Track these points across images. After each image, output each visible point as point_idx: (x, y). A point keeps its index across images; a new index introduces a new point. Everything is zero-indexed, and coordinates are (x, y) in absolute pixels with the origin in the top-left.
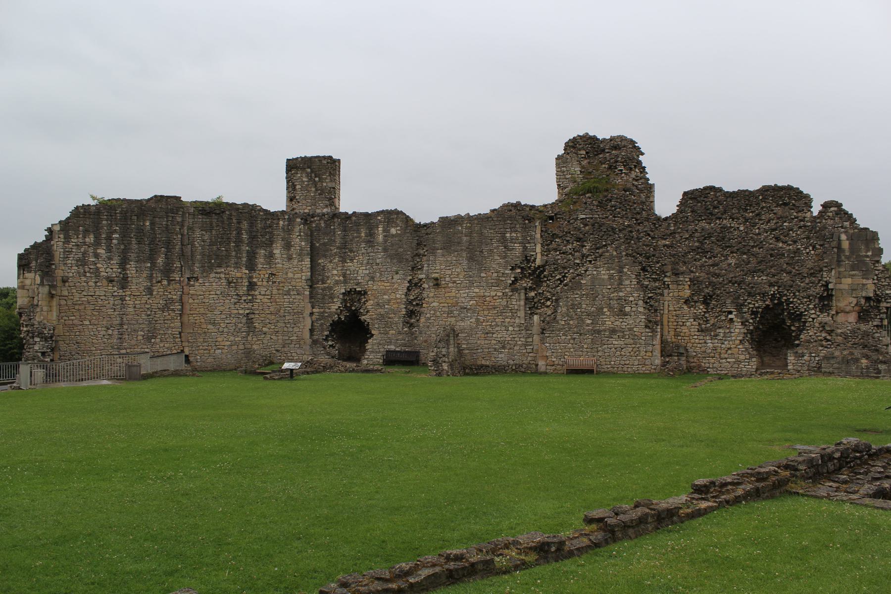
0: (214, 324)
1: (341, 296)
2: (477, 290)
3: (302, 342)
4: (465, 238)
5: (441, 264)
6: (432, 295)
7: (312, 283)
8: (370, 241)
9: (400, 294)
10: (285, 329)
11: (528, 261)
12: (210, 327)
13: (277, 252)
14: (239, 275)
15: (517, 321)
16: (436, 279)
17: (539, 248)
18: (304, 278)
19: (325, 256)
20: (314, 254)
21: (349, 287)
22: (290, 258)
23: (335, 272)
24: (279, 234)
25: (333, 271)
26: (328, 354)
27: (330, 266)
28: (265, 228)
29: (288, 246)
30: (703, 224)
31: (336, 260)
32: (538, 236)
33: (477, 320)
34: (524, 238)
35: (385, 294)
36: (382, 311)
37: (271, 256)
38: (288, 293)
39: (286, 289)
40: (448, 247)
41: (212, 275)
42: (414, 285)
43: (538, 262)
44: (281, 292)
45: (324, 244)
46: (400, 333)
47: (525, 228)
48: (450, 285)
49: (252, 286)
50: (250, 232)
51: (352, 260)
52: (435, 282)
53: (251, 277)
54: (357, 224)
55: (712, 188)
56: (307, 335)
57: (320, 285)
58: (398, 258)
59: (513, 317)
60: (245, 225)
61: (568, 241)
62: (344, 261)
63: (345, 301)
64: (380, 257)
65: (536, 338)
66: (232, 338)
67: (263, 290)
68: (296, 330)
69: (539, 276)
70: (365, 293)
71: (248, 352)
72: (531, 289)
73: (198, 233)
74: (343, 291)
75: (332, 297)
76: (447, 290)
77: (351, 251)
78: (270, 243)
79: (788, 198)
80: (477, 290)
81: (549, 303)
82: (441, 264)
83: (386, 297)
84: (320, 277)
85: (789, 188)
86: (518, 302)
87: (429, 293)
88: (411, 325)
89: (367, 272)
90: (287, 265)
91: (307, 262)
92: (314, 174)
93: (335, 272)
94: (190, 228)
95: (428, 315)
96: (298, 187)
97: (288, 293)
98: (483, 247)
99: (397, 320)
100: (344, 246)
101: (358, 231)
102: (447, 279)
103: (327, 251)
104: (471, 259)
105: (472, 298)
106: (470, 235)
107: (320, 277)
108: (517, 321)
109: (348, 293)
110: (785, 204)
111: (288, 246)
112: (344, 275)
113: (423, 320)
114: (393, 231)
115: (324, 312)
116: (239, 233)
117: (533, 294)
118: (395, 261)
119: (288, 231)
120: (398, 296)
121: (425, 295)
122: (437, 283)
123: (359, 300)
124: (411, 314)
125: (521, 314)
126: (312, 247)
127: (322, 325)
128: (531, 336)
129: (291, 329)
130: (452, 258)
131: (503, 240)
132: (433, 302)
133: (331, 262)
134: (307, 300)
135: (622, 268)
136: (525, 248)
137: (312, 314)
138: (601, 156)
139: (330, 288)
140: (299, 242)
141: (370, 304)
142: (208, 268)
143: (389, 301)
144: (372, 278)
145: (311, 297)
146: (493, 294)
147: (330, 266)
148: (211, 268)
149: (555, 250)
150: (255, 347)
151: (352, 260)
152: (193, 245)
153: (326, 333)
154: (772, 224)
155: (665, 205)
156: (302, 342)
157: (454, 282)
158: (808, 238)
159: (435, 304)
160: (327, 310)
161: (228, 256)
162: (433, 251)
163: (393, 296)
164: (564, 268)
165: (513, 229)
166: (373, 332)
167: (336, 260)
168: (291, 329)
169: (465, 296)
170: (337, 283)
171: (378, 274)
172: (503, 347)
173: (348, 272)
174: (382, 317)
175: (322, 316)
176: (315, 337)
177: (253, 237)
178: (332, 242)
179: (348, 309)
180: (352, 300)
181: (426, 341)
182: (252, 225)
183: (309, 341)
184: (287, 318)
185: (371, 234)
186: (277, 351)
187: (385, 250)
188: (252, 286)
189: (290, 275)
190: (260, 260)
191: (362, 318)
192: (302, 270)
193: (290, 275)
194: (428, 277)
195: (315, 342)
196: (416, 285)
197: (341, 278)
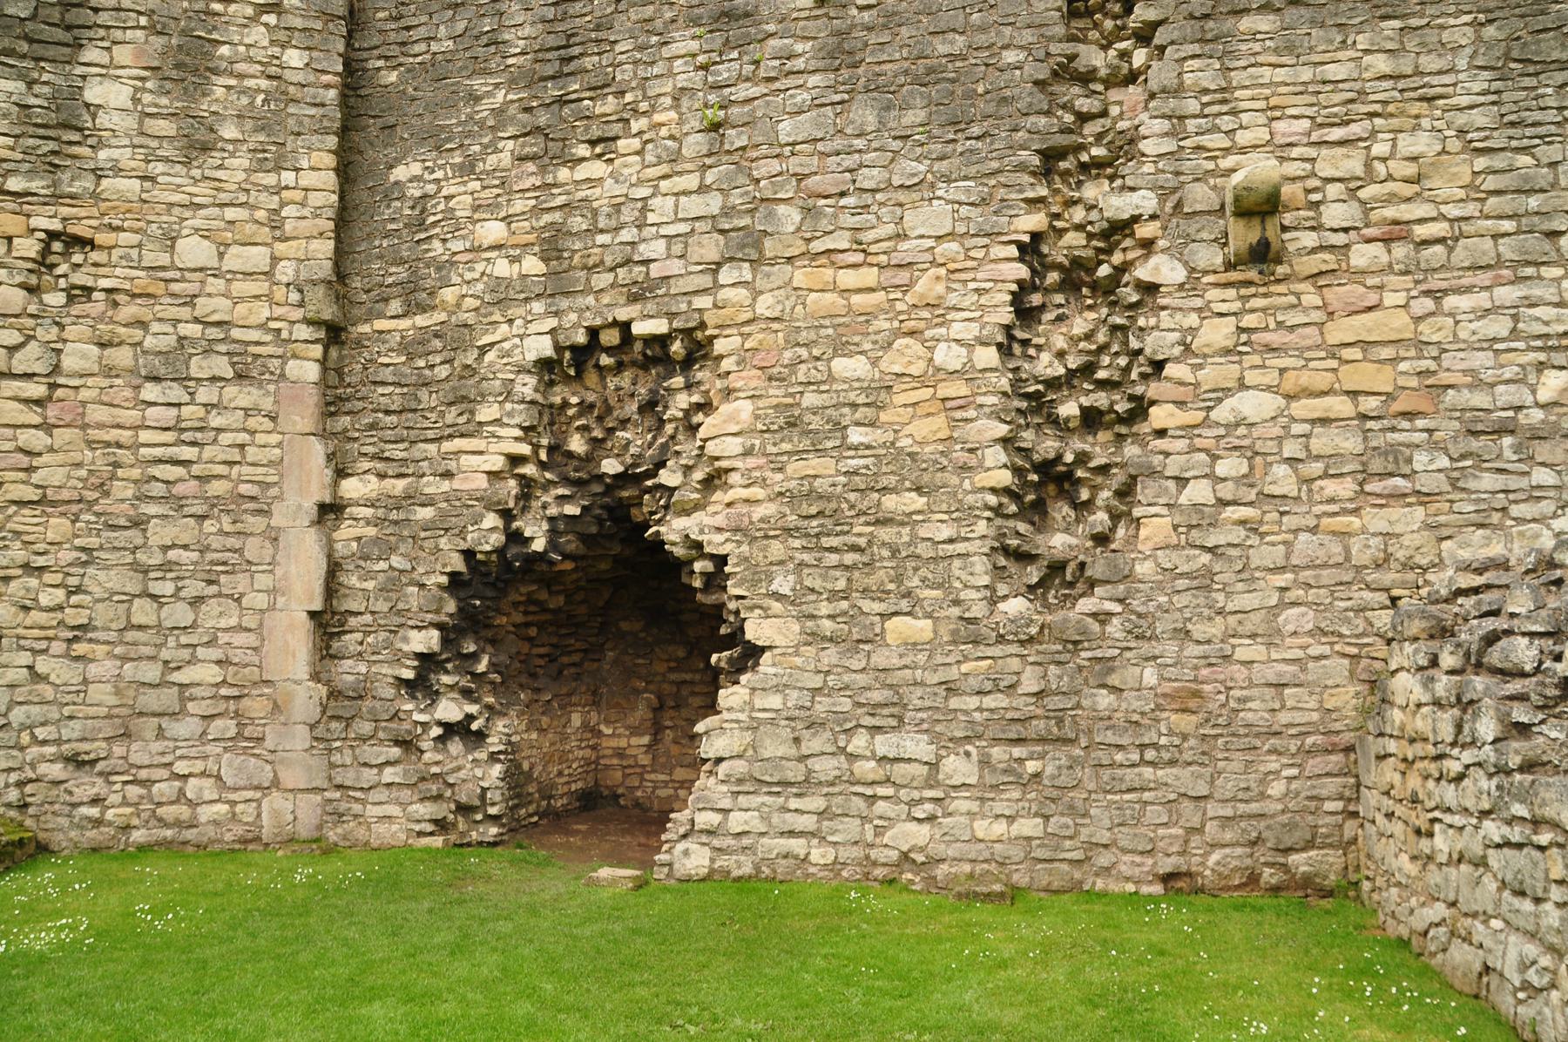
1: (527, 386)
3: (256, 706)
5: (1274, 113)
6: (1217, 333)
9: (965, 342)
10: (143, 612)
13: (110, 96)
18: (286, 271)
19: (436, 140)
20: (359, 125)
22: (198, 145)
23: (493, 231)
26: (430, 785)
27: (462, 195)
29: (188, 63)
35: (842, 348)
38: (171, 368)
39: (159, 339)
42: (1070, 273)
44: (122, 357)
45: (436, 70)
46: (970, 633)
48: (1363, 255)
51: (603, 144)
52: (1243, 235)
57: (393, 324)
62: (549, 149)
63: (551, 416)
68: (216, 616)
70: (699, 350)
76: (1344, 293)
82: (1274, 113)
83: (850, 367)
84: (401, 273)
89: (714, 203)
90: (175, 184)
91: (315, 174)
93: (493, 231)
95: (1199, 492)
97: (171, 368)
102: (1335, 214)
107: (401, 273)
109: (574, 361)
111: (188, 63)
112: (552, 246)
113: (1156, 527)
115: (412, 498)
118: (914, 116)
120: (948, 356)
122: (1260, 233)
124: (1045, 485)
126: (353, 78)
129: (180, 614)
133: (467, 169)
134: (302, 417)
137: (330, 511)
139: (456, 337)
141: (727, 430)
143: (878, 392)
144: (747, 246)
145: (335, 398)
147: (462, 195)
151: (603, 144)
153: (426, 640)
156: (256, 706)
157: (1396, 232)
159: (1254, 405)
160: (433, 486)
163: (906, 356)
166: (754, 631)
168: (180, 614)
170: (502, 296)
171: (789, 216)
173: (578, 223)
174: (817, 518)
176: (348, 671)
179: (578, 475)
181: (1187, 699)
183: (306, 698)
184: (159, 533)
186: (76, 762)
189: (194, 251)
191: (673, 530)
192: (275, 222)
193: (194, 251)
195: (341, 704)
196: (1076, 276)
197: (533, 265)
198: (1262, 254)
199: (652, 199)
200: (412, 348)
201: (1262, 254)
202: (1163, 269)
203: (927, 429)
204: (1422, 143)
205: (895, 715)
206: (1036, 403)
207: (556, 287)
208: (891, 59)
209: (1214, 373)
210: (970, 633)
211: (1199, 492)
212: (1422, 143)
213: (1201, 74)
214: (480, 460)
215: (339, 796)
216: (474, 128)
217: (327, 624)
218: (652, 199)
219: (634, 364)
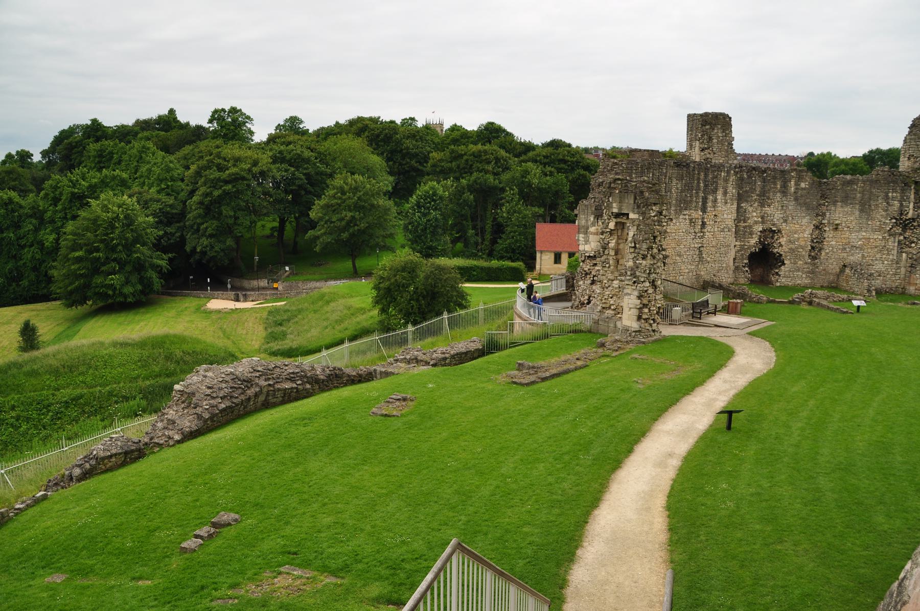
0: (680, 256)
4: (859, 195)
7: (738, 220)
8: (784, 191)
9: (807, 234)
11: (901, 214)
12: (678, 258)
14: (696, 216)
15: (891, 257)
16: (837, 225)
17: (911, 206)
19: (747, 201)
20: (740, 198)
21: (768, 225)
22: (726, 203)
24: (721, 182)
25: (753, 214)
28: (713, 178)
32: (912, 196)
33: (863, 256)
34: (902, 197)
36: (793, 246)
37: (715, 201)
41: (681, 217)
43: (910, 215)
45: (746, 191)
46: (806, 263)
47: (903, 191)
49: (704, 224)
50: (705, 181)
53: (703, 218)
54: (775, 178)
56: (731, 263)
58: (808, 207)
59: (888, 254)
60: (702, 176)
62: (762, 205)
64: (792, 205)
65: (903, 270)
66: (689, 267)
67: (708, 228)
69: (906, 225)
71: (698, 276)
72: (901, 234)
73: (674, 181)
74: (761, 229)
75: (751, 233)
77: (769, 198)
78: (715, 191)
81: (913, 245)
83: (796, 236)
86: (892, 244)
87: (829, 234)
88: (814, 258)
90: (724, 208)
91: (735, 206)
92: (710, 127)
93: (755, 214)
94: (670, 178)
96: (715, 141)
97: (723, 230)
99: (805, 254)
100: (763, 194)
101: (775, 184)
103: (749, 197)
104: (861, 211)
105: (860, 239)
108: (891, 257)
111: (725, 193)
112: (762, 218)
113: (823, 254)
114: (803, 185)
116: (699, 183)
117: (902, 238)
119: (726, 181)
121: (826, 236)
123: (772, 238)
125: (895, 252)
127: (742, 255)
128: (899, 268)
130: (848, 209)
131: (887, 198)
132: (832, 241)
136: (901, 205)
139: (750, 227)
140: (732, 190)
141: (783, 241)
142: (679, 211)
143: (799, 239)
144: (785, 221)
145: (736, 233)
146: (876, 237)
147: (750, 209)
148: (681, 211)
150: (702, 273)
152: (671, 192)
159: (833, 243)
161: (691, 201)
165: (894, 191)
169: (856, 238)
170: (756, 223)
172: (880, 276)
174: (792, 251)
175: (742, 248)
177: (706, 186)
178: (753, 190)
180: (766, 238)
182: (706, 175)
183: (733, 268)
185: (785, 186)
187: (796, 199)
188: (704, 224)
190: (710, 204)
194: (829, 223)
195: (737, 268)
199: (775, 213)
200: (744, 227)
201: (836, 229)
202: (827, 229)
203: (803, 243)
205: (799, 270)
206: (812, 241)
207: (763, 222)
208: (802, 201)
210: (806, 263)
213: (833, 208)
214: (754, 241)
215: (736, 279)
216: (752, 201)
217: (734, 259)
218: (775, 213)
219: (771, 233)
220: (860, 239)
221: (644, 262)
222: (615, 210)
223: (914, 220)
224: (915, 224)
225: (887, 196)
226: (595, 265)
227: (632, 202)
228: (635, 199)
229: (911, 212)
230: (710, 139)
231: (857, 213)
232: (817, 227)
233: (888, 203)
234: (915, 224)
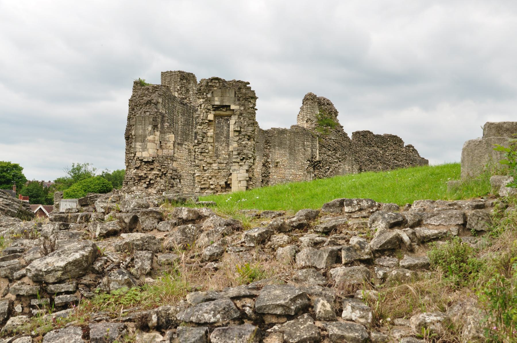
2: (293, 171)
4: (288, 142)
6: (273, 171)
16: (277, 163)
23: (224, 152)
27: (221, 148)
30: (367, 148)
31: (224, 145)
32: (318, 145)
40: (281, 144)
48: (282, 167)
55: (369, 132)
61: (329, 150)
66: (188, 190)
79: (396, 140)
80: (293, 171)
85: (395, 137)
87: (272, 170)
95: (272, 183)
96: (191, 92)
98: (296, 148)
104: (290, 154)
105: (291, 175)
106: (290, 140)
110: (395, 144)
120: (258, 170)
130: (282, 152)
133: (221, 145)
135: (353, 166)
136: (312, 151)
138: (323, 107)
146: (300, 173)
147: (221, 148)
149: (324, 154)
154: (393, 152)
155: (350, 136)
158: (406, 160)
159: (275, 177)
162: (275, 146)
164: (331, 163)
167: (224, 145)
169: (289, 173)
197: (227, 156)
198: (277, 166)
201: (277, 166)
202: (271, 166)
204: (285, 159)
209: (273, 174)
211: (272, 183)
212: (285, 159)
220: (291, 175)
221: (250, 143)
222: (217, 103)
223: (320, 162)
224: (321, 165)
225: (304, 144)
226: (152, 169)
227: (233, 95)
228: (235, 93)
229: (318, 156)
230: (188, 91)
231: (288, 155)
232: (264, 165)
233: (305, 149)
234: (321, 165)
